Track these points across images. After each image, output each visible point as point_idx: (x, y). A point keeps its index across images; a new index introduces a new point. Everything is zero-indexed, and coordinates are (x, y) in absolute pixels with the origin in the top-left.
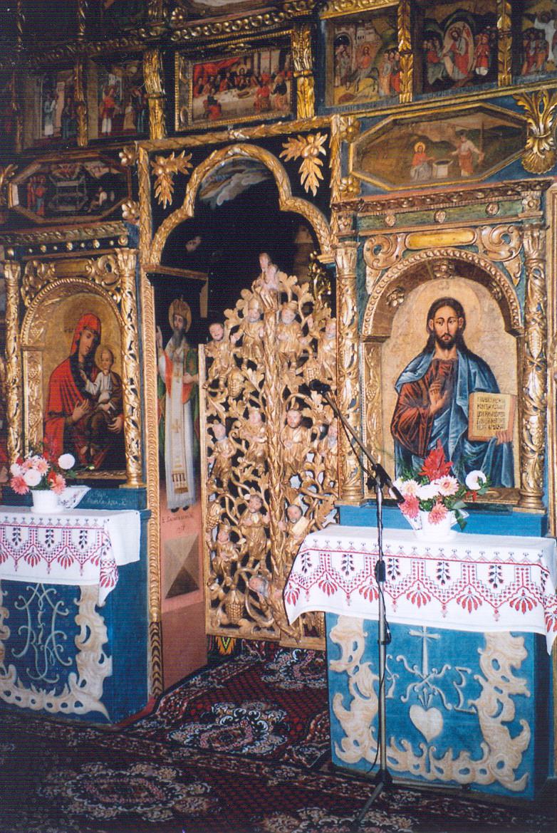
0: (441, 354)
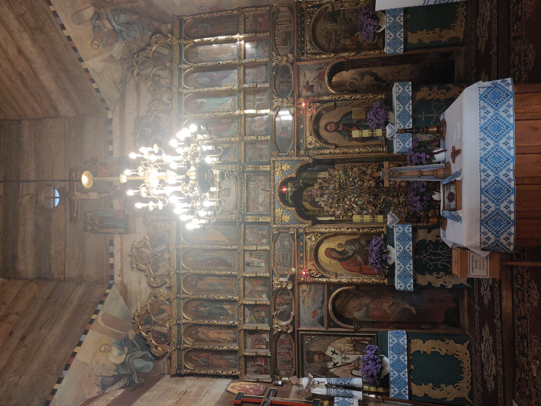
0: (341, 128)
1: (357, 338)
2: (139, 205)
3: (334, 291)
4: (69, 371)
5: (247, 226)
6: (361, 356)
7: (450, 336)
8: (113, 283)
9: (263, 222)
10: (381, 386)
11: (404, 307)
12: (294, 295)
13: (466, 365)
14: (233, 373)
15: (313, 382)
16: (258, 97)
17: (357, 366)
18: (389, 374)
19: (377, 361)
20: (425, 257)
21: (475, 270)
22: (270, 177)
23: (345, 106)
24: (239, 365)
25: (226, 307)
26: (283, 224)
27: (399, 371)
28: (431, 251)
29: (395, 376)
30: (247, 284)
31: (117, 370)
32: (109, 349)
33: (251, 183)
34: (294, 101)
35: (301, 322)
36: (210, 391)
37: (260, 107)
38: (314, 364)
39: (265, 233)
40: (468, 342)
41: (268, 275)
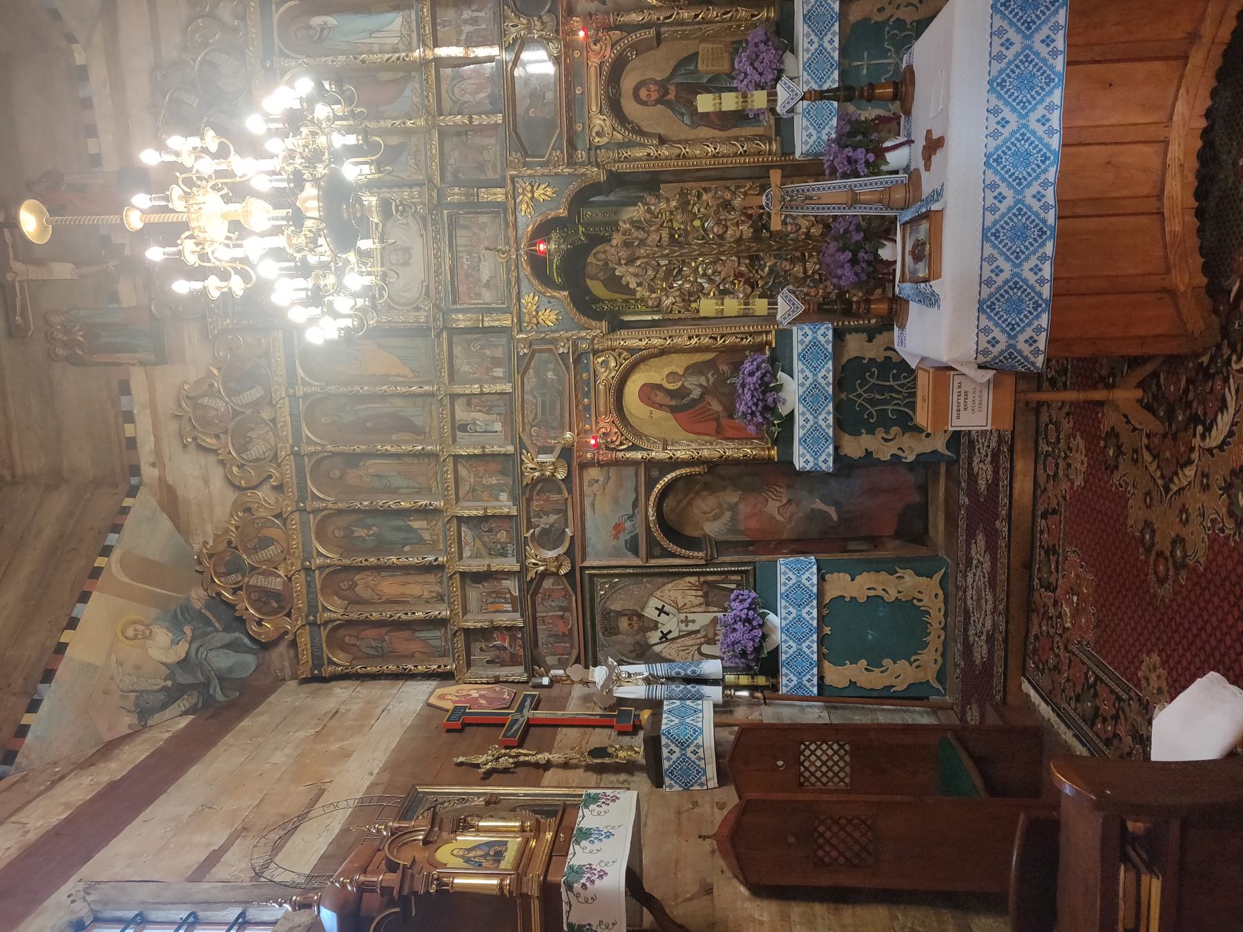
0: (671, 96)
1: (710, 578)
2: (181, 287)
3: (661, 478)
4: (53, 683)
5: (455, 339)
6: (720, 615)
7: (905, 563)
8: (141, 483)
9: (493, 327)
10: (761, 673)
11: (813, 506)
12: (570, 491)
13: (936, 618)
14: (439, 667)
15: (618, 676)
16: (467, 14)
17: (710, 635)
18: (778, 647)
19: (755, 623)
20: (859, 396)
21: (962, 412)
22: (505, 219)
23: (682, 38)
24: (453, 650)
25: (417, 524)
26: (541, 332)
27: (799, 641)
28: (873, 381)
29: (791, 652)
30: (463, 472)
31: (171, 676)
32: (147, 632)
33: (459, 232)
34: (558, 25)
35: (589, 549)
36: (389, 707)
37: (474, 39)
38: (619, 637)
39: (499, 353)
40: (943, 571)
41: (510, 449)
